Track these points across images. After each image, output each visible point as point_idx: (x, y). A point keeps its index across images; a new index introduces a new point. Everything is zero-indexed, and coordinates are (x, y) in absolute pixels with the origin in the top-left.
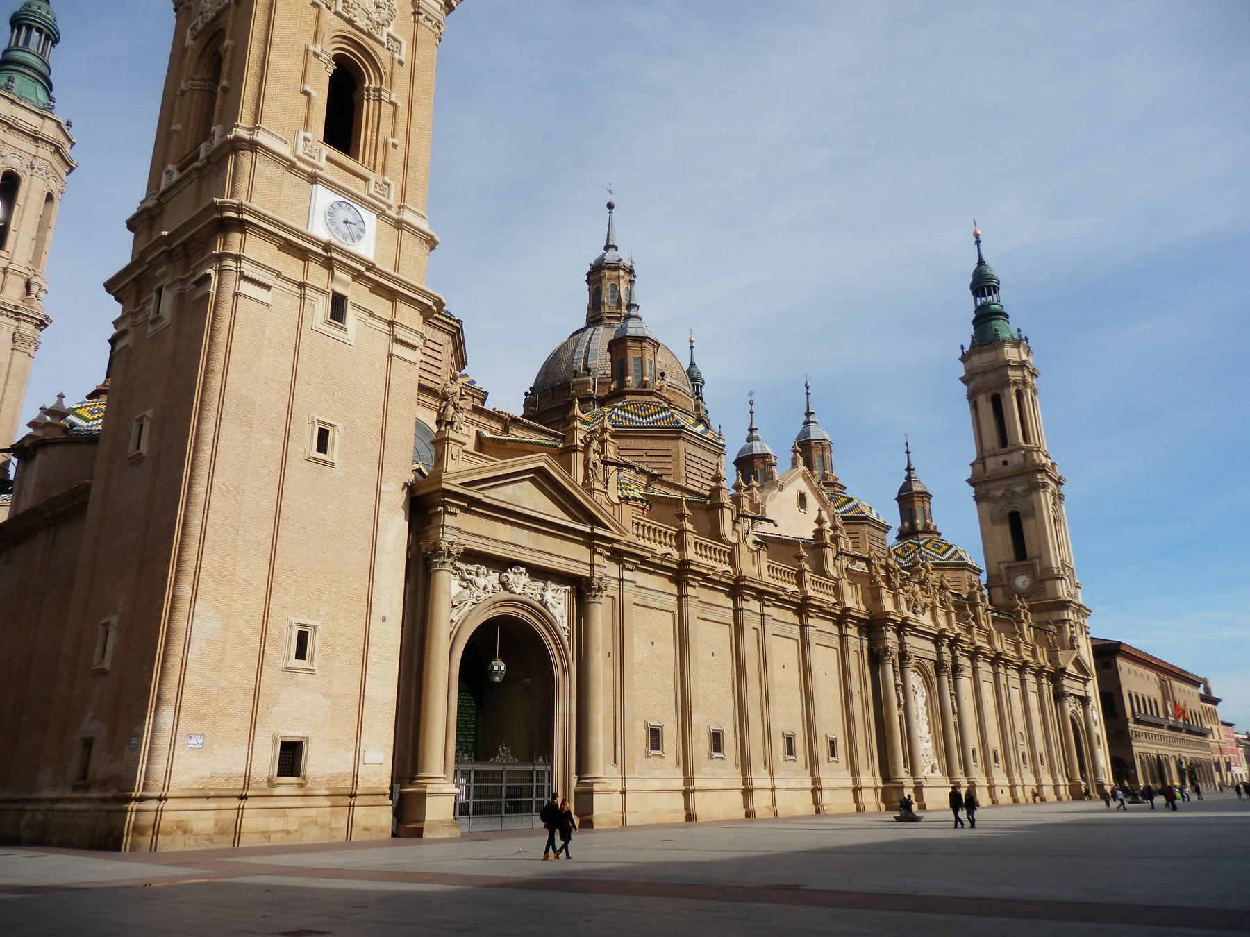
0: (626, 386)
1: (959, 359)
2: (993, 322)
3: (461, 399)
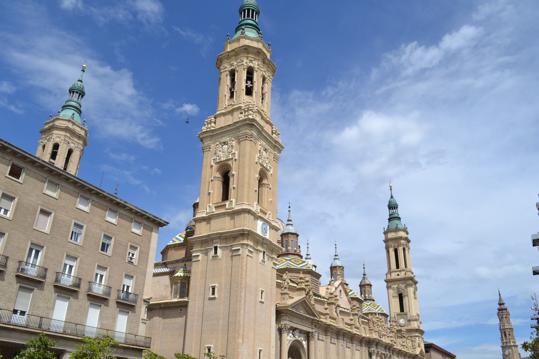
2: (396, 221)
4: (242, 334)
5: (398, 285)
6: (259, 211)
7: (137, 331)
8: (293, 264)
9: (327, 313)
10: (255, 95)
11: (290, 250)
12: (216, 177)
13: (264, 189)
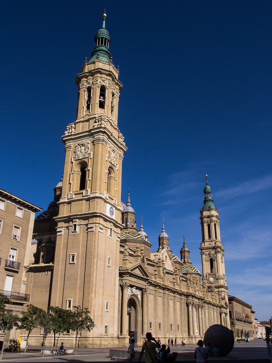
6: (108, 198)
7: (20, 291)
8: (131, 236)
10: (106, 108)
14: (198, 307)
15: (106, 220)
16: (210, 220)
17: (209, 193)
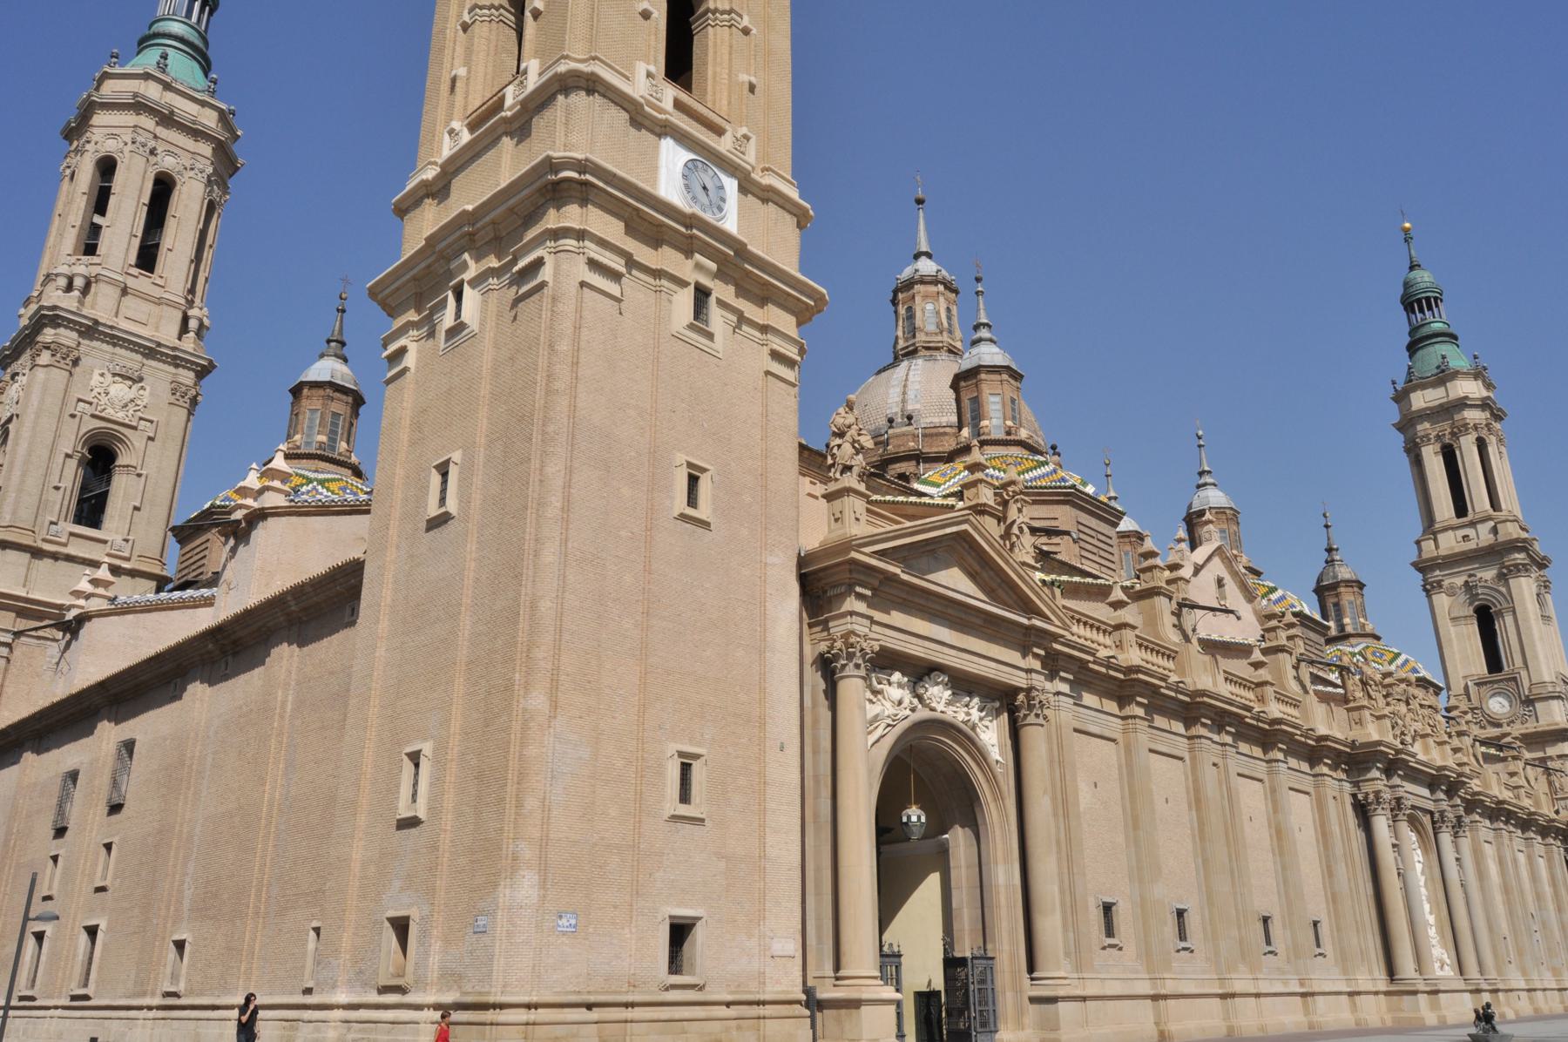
0: (983, 434)
1: (1392, 398)
2: (1437, 346)
3: (859, 435)
4: (549, 667)
5: (1470, 576)
6: (668, 104)
9: (1123, 621)
11: (986, 430)
12: (481, 8)
13: (715, 35)
14: (1429, 827)
15: (655, 237)
16: (1453, 423)
17: (1430, 308)
